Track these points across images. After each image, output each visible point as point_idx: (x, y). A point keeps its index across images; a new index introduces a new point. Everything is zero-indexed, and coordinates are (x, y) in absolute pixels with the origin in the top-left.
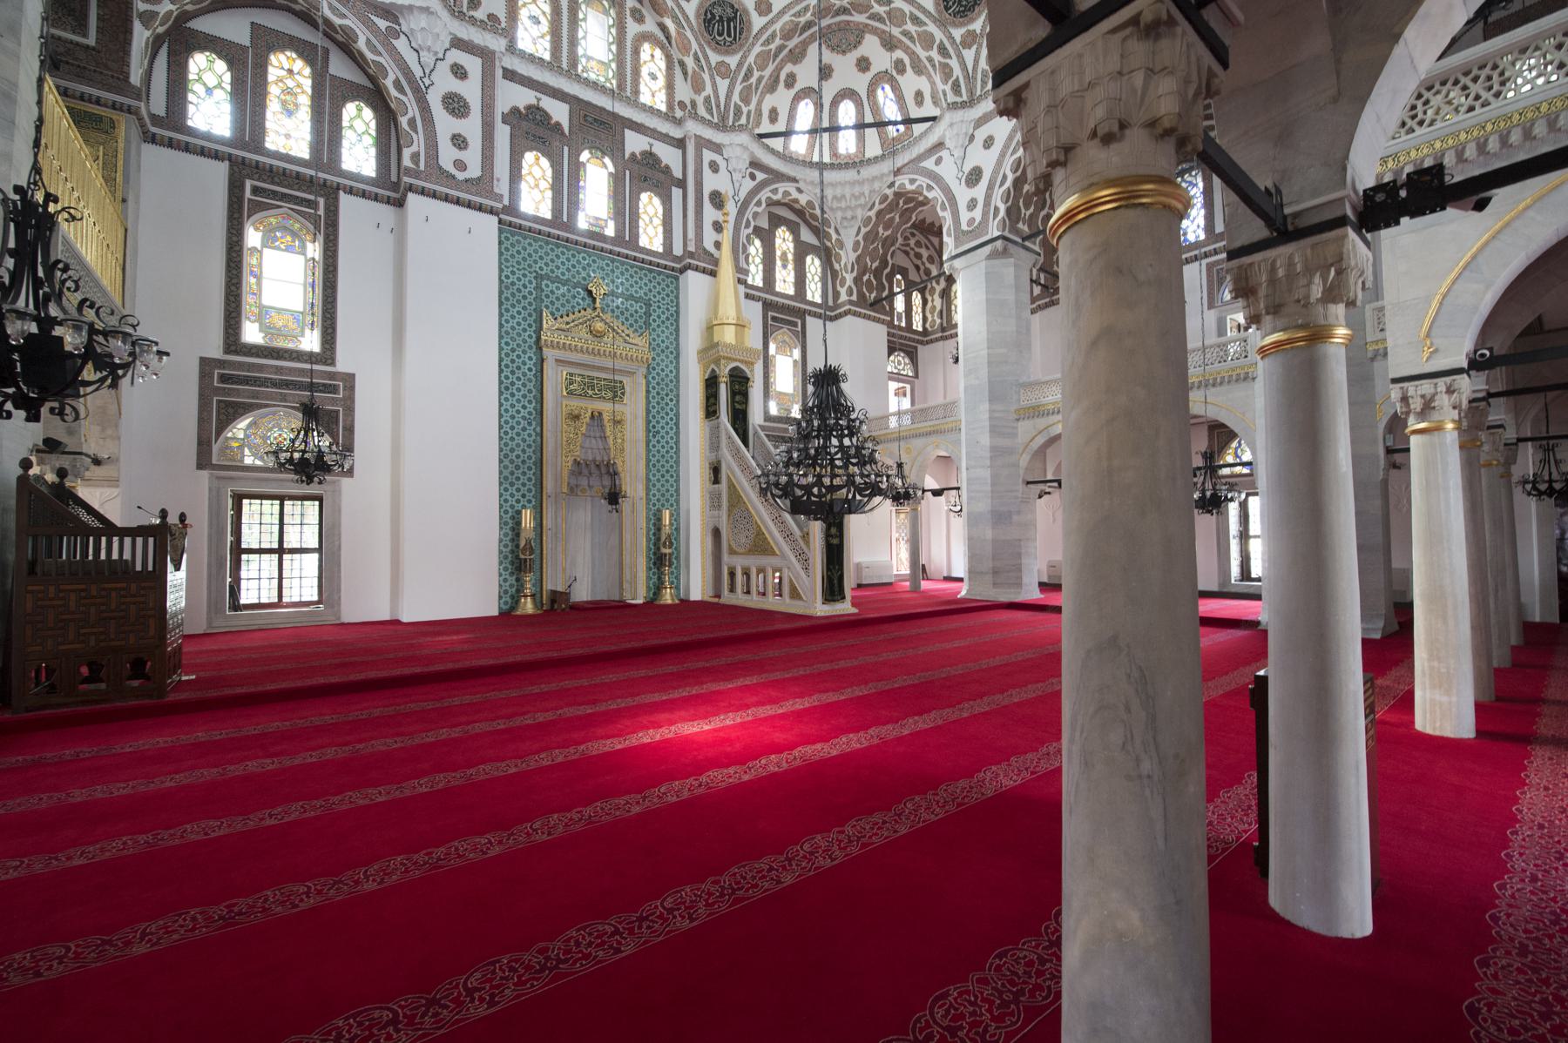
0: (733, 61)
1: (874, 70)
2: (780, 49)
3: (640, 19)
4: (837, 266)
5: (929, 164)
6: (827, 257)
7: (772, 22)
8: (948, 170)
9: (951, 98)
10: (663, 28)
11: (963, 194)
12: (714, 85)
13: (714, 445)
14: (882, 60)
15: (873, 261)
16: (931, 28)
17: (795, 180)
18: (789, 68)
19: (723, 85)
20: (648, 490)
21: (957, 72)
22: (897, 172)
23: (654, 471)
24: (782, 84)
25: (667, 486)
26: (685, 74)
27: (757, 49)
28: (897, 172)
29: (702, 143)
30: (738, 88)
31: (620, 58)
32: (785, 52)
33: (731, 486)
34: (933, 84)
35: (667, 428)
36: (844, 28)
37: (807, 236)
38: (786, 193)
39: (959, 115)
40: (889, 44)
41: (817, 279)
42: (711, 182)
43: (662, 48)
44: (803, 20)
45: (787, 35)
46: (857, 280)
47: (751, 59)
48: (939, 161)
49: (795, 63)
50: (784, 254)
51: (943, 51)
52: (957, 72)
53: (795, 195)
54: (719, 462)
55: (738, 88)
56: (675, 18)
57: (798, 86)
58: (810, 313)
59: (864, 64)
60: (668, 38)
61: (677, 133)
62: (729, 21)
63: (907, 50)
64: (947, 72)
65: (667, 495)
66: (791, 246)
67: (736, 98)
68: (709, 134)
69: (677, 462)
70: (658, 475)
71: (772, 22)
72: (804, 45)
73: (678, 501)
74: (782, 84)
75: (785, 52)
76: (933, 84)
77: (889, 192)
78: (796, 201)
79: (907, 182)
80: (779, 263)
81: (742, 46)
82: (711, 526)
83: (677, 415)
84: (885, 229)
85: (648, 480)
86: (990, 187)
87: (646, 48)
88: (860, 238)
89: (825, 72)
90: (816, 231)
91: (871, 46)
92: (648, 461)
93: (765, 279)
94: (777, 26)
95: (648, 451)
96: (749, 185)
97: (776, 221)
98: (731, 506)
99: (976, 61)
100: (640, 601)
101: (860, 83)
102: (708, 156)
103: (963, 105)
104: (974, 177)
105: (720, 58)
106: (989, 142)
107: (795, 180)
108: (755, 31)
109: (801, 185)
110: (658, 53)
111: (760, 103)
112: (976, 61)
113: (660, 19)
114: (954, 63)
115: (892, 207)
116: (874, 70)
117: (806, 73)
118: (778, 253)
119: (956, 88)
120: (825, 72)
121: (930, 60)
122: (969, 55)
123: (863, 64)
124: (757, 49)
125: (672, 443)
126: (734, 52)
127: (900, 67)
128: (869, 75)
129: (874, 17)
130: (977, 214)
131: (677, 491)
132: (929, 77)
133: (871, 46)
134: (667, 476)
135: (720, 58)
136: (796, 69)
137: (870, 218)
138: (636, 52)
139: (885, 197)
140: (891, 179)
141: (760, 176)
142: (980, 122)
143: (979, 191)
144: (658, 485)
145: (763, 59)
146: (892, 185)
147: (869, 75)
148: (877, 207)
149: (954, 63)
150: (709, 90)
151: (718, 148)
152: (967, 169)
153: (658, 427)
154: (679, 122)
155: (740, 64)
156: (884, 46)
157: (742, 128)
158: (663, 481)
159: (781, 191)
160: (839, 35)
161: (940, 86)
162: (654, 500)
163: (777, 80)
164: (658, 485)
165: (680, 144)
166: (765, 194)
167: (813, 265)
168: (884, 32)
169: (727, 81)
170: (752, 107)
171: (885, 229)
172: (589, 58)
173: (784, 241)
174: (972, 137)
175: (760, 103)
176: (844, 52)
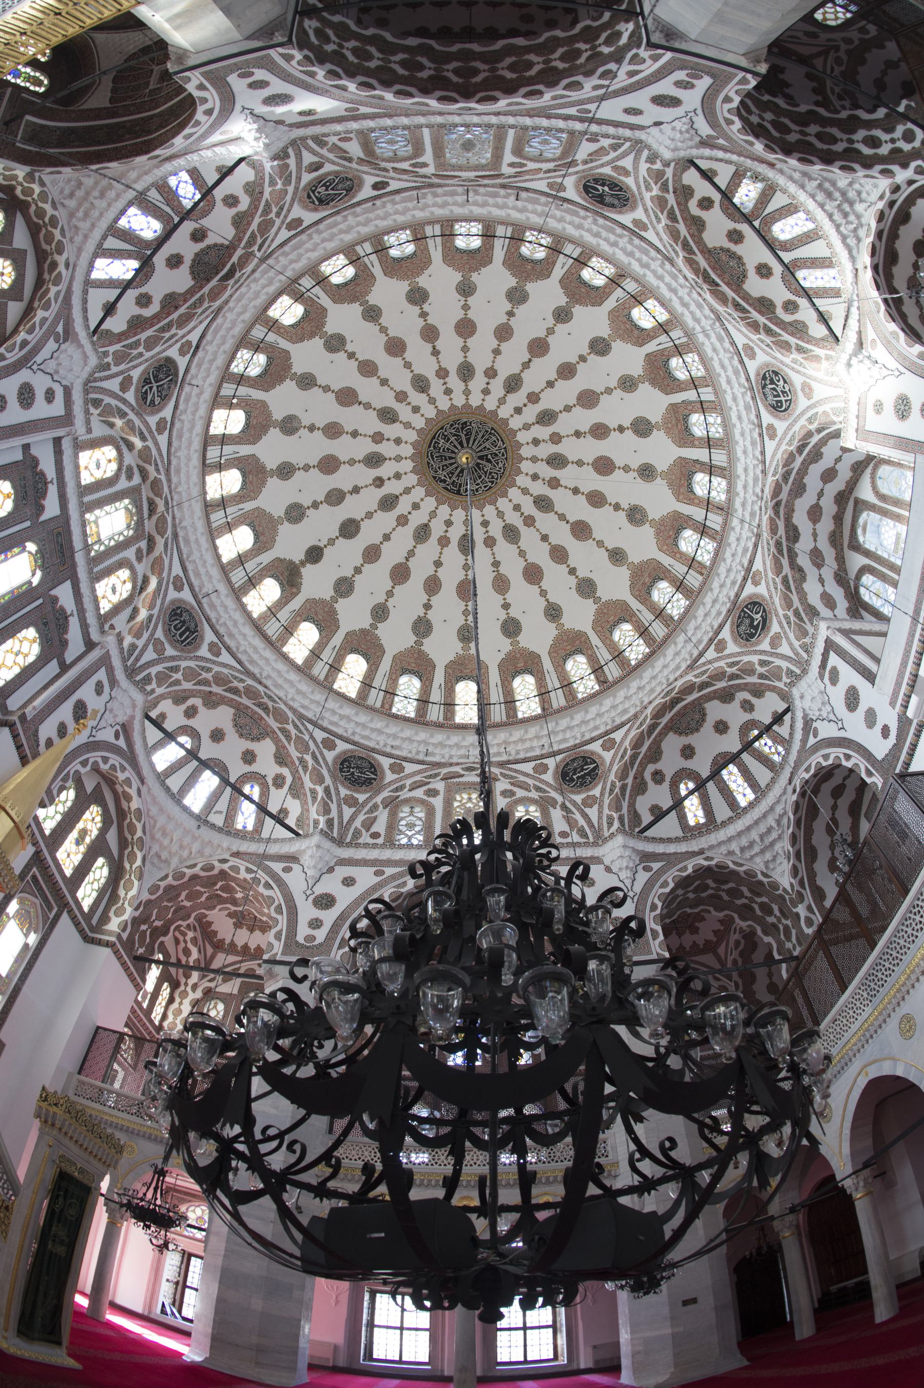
0: (170, 651)
1: (254, 768)
2: (206, 682)
3: (139, 559)
4: (122, 892)
5: (277, 867)
6: (117, 874)
7: (214, 662)
8: (296, 881)
9: (322, 825)
10: (146, 581)
11: (307, 911)
12: (146, 646)
14: (266, 765)
15: (158, 918)
16: (325, 772)
17: (142, 781)
18: (197, 702)
19: (150, 655)
21: (334, 814)
22: (237, 854)
24: (183, 707)
26: (132, 618)
27: (192, 664)
28: (237, 854)
29: (105, 661)
30: (159, 668)
31: (110, 552)
32: (207, 689)
34: (305, 810)
36: (257, 720)
37: (112, 837)
38: (128, 782)
39: (327, 844)
40: (281, 758)
41: (96, 886)
42: (86, 692)
43: (134, 588)
44: (236, 684)
45: (219, 680)
46: (136, 922)
47: (184, 664)
48: (287, 870)
49: (205, 705)
50: (84, 833)
51: (327, 791)
52: (334, 814)
53: (133, 792)
55: (159, 668)
56: (159, 584)
57: (191, 722)
58: (70, 912)
59: (249, 757)
60: (142, 589)
61: (95, 636)
62: (187, 629)
63: (295, 773)
64: (327, 811)
66: (95, 833)
67: (154, 671)
68: (116, 662)
71: (214, 662)
72: (222, 701)
74: (183, 707)
75: (207, 689)
76: (305, 810)
77: (216, 864)
78: (129, 798)
79: (242, 869)
80: (74, 835)
81: (182, 650)
84: (188, 898)
86: (342, 918)
87: (124, 574)
88: (163, 884)
89: (217, 736)
90: (123, 843)
91: (265, 749)
93: (54, 831)
94: (216, 669)
96: (107, 735)
97: (97, 798)
99: (352, 819)
101: (236, 770)
102: (101, 675)
103: (333, 840)
104: (325, 901)
105: (163, 639)
106: (349, 882)
107: (142, 781)
108: (199, 654)
109: (144, 790)
110: (129, 586)
111: (162, 697)
112: (352, 819)
113: (149, 574)
114: (334, 807)
115: (210, 882)
116: (254, 768)
117: (206, 720)
118: (80, 825)
119: (330, 823)
120: (217, 736)
121: (313, 792)
122: (348, 812)
123: (249, 757)
124: (192, 664)
126: (175, 648)
127: (279, 781)
128: (247, 769)
129: (284, 731)
130: (320, 935)
132: (304, 804)
133: (265, 749)
135: (163, 639)
136: (202, 709)
137: (183, 875)
138: (120, 565)
139: (212, 868)
140: (227, 856)
141: (122, 743)
142: (343, 862)
143: (329, 917)
145: (190, 674)
146: (224, 861)
147: (247, 769)
148: (197, 870)
149: (334, 807)
150: (140, 643)
151: (113, 682)
152: (319, 890)
154: (103, 632)
155: (173, 658)
156: (276, 757)
157: (142, 690)
159: (127, 774)
160: (248, 720)
161: (313, 815)
163: (184, 699)
165: (90, 645)
166: (115, 760)
167: (100, 871)
168: (284, 747)
169: (155, 656)
170: (160, 691)
171: (188, 898)
172: (96, 522)
173: (92, 820)
174: (331, 870)
175: (162, 697)
176: (241, 736)
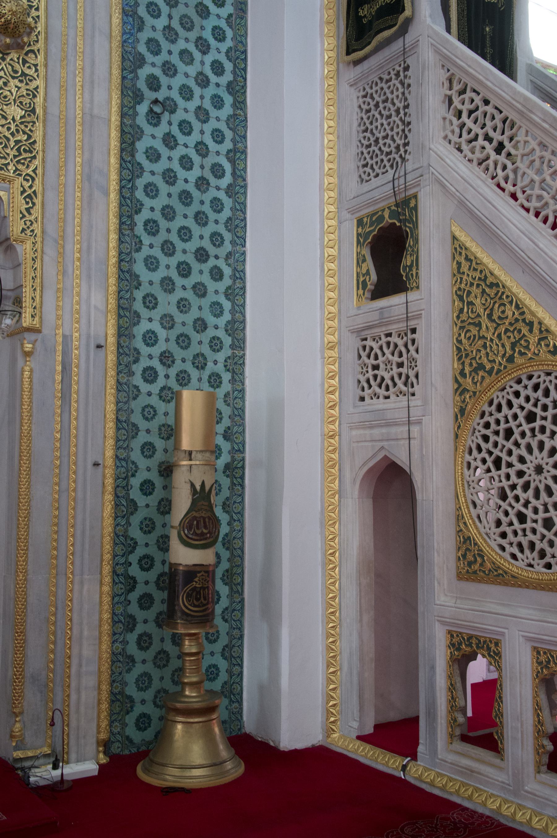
13: (382, 137)
20: (126, 317)
23: (150, 246)
25: (199, 308)
33: (475, 287)
35: (202, 97)
54: (406, 207)
65: (200, 343)
69: (237, 225)
70: (168, 266)
73: (236, 366)
82: (363, 457)
83: (239, 55)
85: (127, 279)
92: (128, 208)
95: (129, 169)
98: (470, 368)
100: (83, 766)
125: (219, 153)
131: (237, 328)
134: (200, 273)
144: (167, 303)
153: (170, 87)
158: (183, 288)
162: (149, 355)
164: (167, 303)
